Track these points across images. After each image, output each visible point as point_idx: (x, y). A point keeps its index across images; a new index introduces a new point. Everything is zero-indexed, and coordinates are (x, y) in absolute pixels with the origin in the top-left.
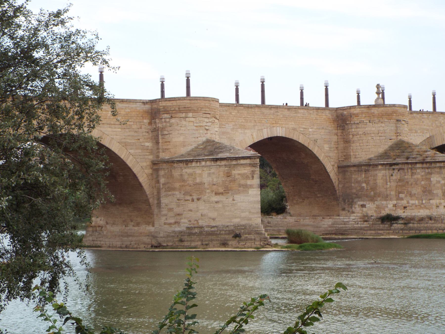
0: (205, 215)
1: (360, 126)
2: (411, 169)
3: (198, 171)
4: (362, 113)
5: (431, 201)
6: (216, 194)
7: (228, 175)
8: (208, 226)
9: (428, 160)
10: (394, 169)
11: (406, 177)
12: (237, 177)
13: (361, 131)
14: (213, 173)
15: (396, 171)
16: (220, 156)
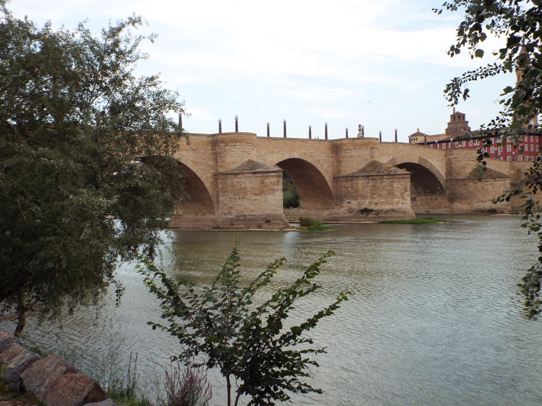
0: (247, 208)
1: (347, 152)
2: (381, 179)
3: (243, 180)
4: (349, 143)
5: (393, 200)
6: (255, 195)
7: (262, 183)
8: (250, 215)
9: (392, 173)
10: (369, 179)
11: (377, 184)
12: (268, 184)
13: (348, 155)
14: (253, 181)
15: (371, 180)
16: (257, 170)
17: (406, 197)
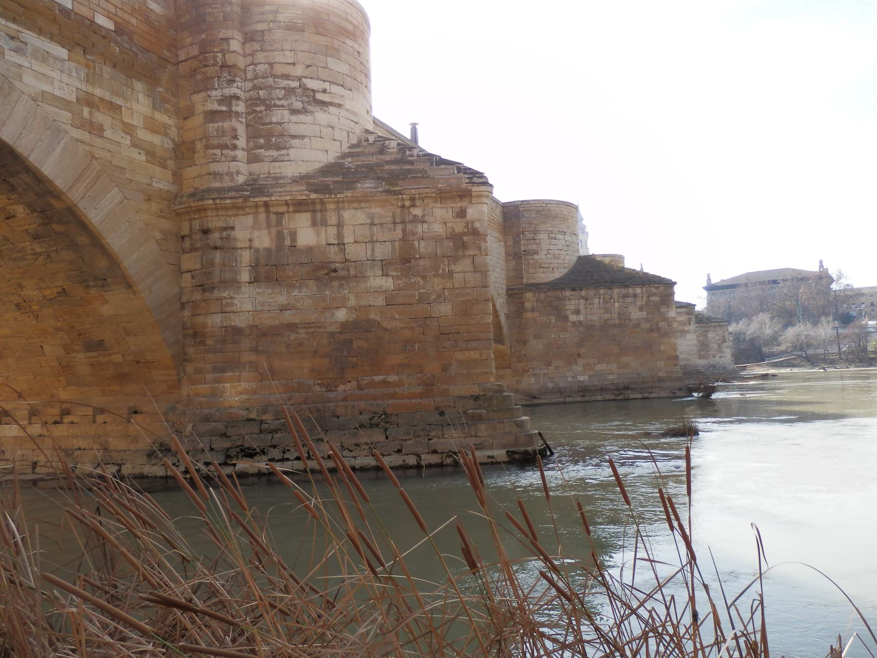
17: (724, 350)
